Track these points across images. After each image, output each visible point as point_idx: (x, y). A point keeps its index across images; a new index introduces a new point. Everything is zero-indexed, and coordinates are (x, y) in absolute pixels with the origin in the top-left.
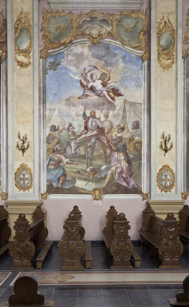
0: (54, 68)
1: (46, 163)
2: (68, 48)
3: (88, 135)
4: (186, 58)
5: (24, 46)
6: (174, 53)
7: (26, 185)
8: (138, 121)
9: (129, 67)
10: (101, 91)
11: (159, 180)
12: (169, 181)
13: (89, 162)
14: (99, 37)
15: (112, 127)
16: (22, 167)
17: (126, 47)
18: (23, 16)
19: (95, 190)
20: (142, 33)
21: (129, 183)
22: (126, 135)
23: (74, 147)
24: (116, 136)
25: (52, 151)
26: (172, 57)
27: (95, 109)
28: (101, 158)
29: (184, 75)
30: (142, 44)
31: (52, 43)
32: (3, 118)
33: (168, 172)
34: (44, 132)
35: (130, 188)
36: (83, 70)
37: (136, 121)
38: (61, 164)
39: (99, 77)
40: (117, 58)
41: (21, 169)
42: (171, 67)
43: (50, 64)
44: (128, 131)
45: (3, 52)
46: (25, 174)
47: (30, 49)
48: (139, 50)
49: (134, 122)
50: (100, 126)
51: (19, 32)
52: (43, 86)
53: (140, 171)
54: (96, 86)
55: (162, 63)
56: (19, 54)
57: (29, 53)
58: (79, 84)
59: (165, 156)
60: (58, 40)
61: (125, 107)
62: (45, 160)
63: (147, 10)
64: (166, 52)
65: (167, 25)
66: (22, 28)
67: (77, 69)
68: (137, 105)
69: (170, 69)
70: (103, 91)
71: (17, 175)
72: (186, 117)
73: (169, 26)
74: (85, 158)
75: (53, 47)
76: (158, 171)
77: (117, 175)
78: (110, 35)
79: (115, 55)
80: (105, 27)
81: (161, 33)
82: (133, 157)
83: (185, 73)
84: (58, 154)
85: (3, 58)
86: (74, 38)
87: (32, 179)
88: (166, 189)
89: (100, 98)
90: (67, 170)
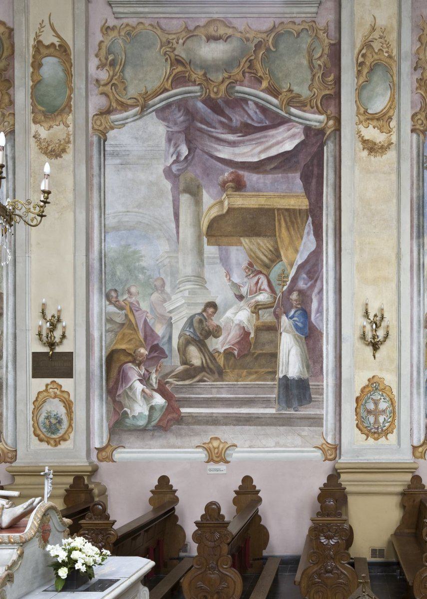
5: (378, 105)
16: (373, 384)
18: (376, 35)
32: (327, 270)
34: (419, 302)
41: (370, 389)
45: (327, 118)
46: (378, 400)
47: (391, 113)
51: (367, 73)
52: (418, 197)
56: (365, 124)
57: (389, 120)
66: (373, 64)
71: (360, 403)
85: (328, 133)
87: (393, 412)
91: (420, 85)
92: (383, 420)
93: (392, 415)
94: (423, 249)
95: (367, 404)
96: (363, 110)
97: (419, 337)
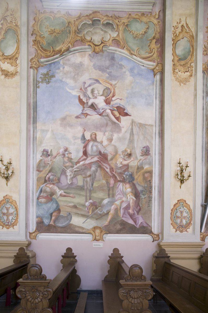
0: (47, 80)
1: (36, 195)
2: (64, 56)
3: (88, 161)
4: (205, 72)
5: (10, 51)
6: (193, 64)
7: (11, 221)
8: (148, 146)
9: (137, 81)
10: (104, 109)
11: (174, 217)
12: (185, 219)
13: (88, 195)
14: (102, 45)
15: (116, 152)
16: (6, 199)
17: (134, 57)
18: (8, 13)
19: (95, 228)
20: (154, 41)
21: (136, 221)
22: (133, 163)
23: (71, 176)
24: (121, 163)
25: (43, 181)
26: (189, 68)
27: (97, 131)
28: (103, 190)
29: (204, 93)
30: (154, 54)
31: (45, 50)
33: (184, 208)
34: (33, 157)
35: (138, 227)
36: (82, 84)
37: (145, 146)
38: (54, 197)
39: (101, 93)
40: (124, 70)
41: (4, 202)
42: (189, 81)
43: (42, 76)
44: (136, 157)
46: (8, 208)
47: (17, 56)
48: (151, 61)
49: (143, 148)
50: (102, 152)
51: (4, 33)
52: (34, 102)
53: (149, 206)
54: (98, 103)
55: (177, 76)
56: (3, 61)
57: (16, 59)
58: (77, 101)
59: (180, 188)
60: (52, 47)
61: (132, 129)
62: (35, 192)
63: (160, 13)
64: (183, 62)
65: (184, 30)
66: (7, 29)
67: (75, 83)
68: (147, 127)
69: (187, 83)
70: (107, 109)
72: (205, 143)
73: (187, 31)
74: (84, 189)
75: (46, 55)
76: (172, 207)
77: (122, 211)
78: (116, 42)
79: (121, 66)
80: (110, 32)
81: (177, 40)
82: (142, 189)
83: (204, 90)
84: (51, 184)
86: (72, 44)
87: (17, 214)
88: (181, 228)
89: (102, 118)
90: (61, 204)
91: (34, 43)
92: (11, 218)
93: (16, 216)
94: (36, 129)
95: (3, 210)
96: (2, 54)
97: (33, 176)
